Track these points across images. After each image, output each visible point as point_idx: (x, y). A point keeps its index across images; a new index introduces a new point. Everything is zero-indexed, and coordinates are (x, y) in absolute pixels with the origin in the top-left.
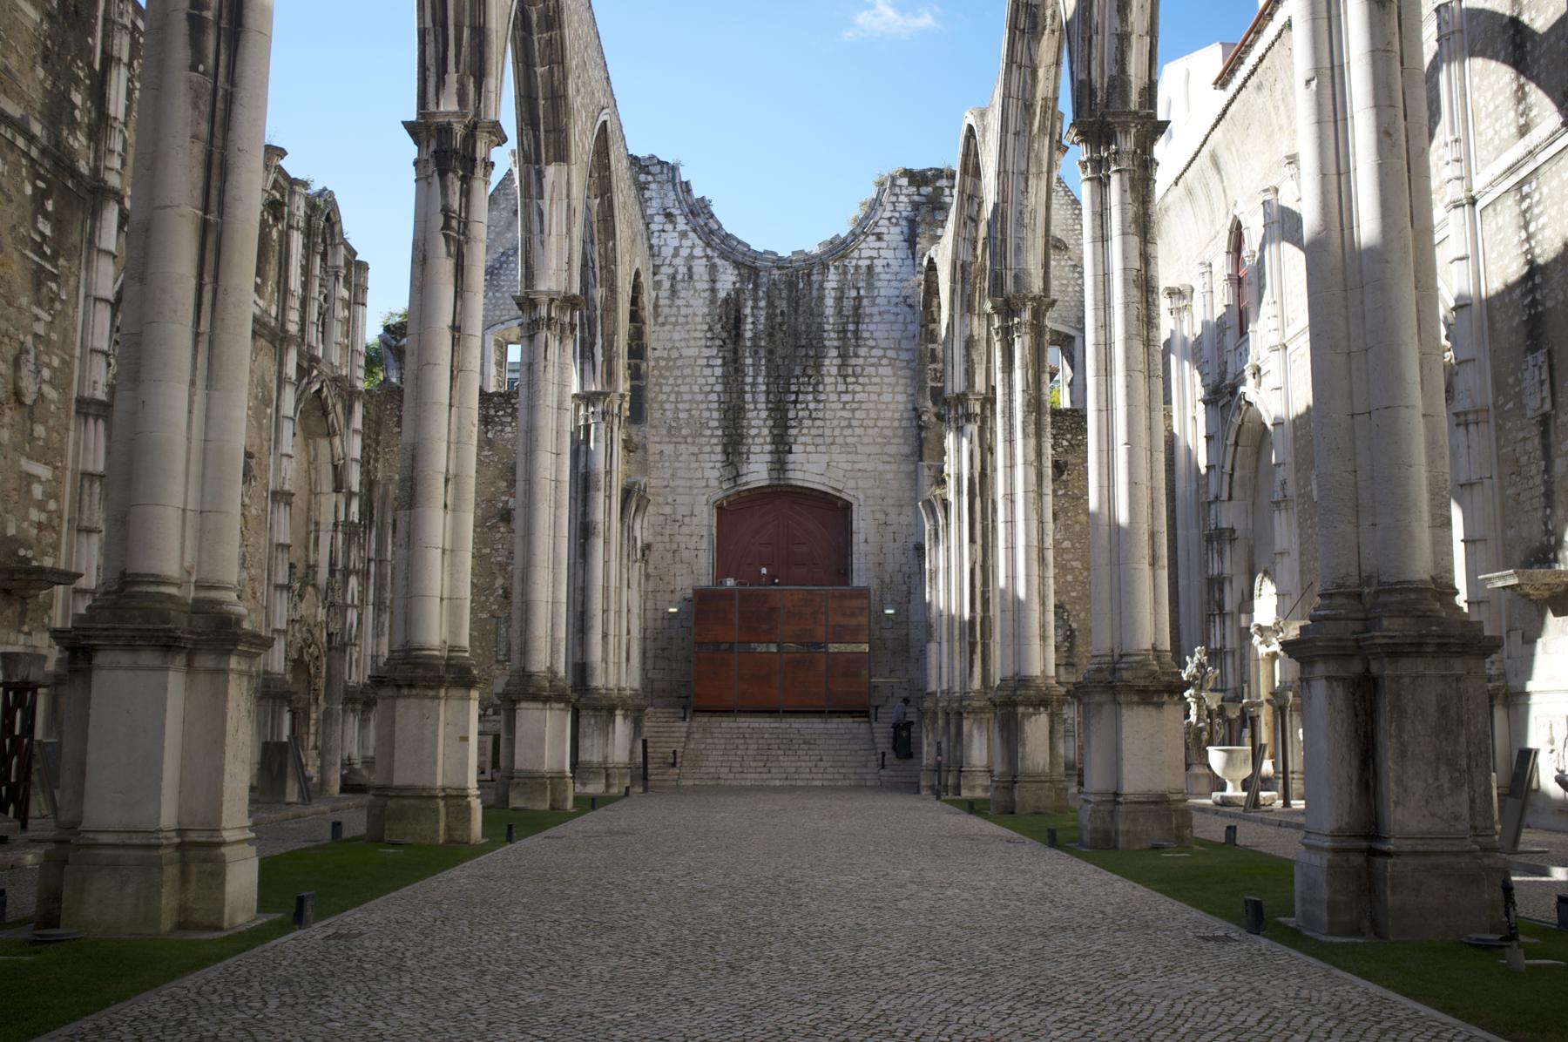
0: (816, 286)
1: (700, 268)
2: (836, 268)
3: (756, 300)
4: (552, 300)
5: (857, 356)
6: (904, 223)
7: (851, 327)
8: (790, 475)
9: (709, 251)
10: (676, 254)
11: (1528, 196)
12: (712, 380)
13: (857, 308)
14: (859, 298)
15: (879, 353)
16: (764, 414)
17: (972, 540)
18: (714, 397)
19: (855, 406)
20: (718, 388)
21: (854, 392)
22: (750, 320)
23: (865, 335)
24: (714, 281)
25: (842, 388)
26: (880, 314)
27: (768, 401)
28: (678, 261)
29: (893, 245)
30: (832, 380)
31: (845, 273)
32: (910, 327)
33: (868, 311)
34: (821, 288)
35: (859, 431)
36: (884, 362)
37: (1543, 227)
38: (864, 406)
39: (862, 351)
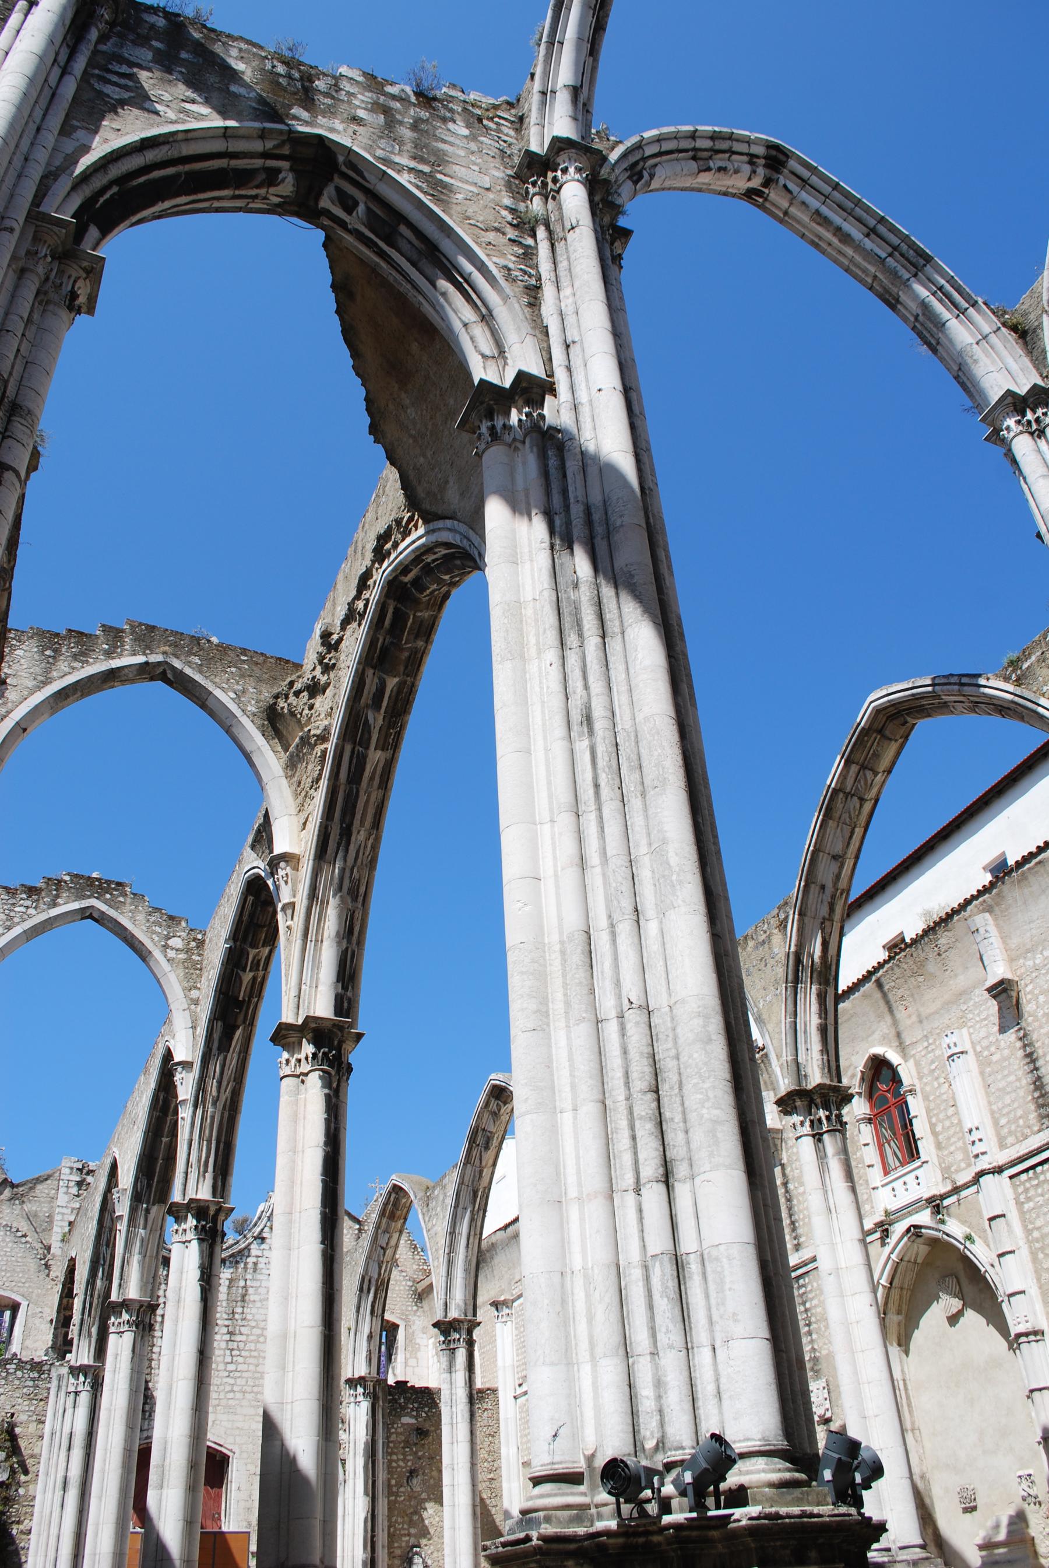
4: (141, 1306)
11: (803, 1286)
13: (244, 1296)
15: (259, 1332)
17: (366, 1493)
21: (237, 1363)
23: (249, 1317)
25: (228, 1359)
30: (222, 1352)
33: (252, 1298)
37: (816, 1306)
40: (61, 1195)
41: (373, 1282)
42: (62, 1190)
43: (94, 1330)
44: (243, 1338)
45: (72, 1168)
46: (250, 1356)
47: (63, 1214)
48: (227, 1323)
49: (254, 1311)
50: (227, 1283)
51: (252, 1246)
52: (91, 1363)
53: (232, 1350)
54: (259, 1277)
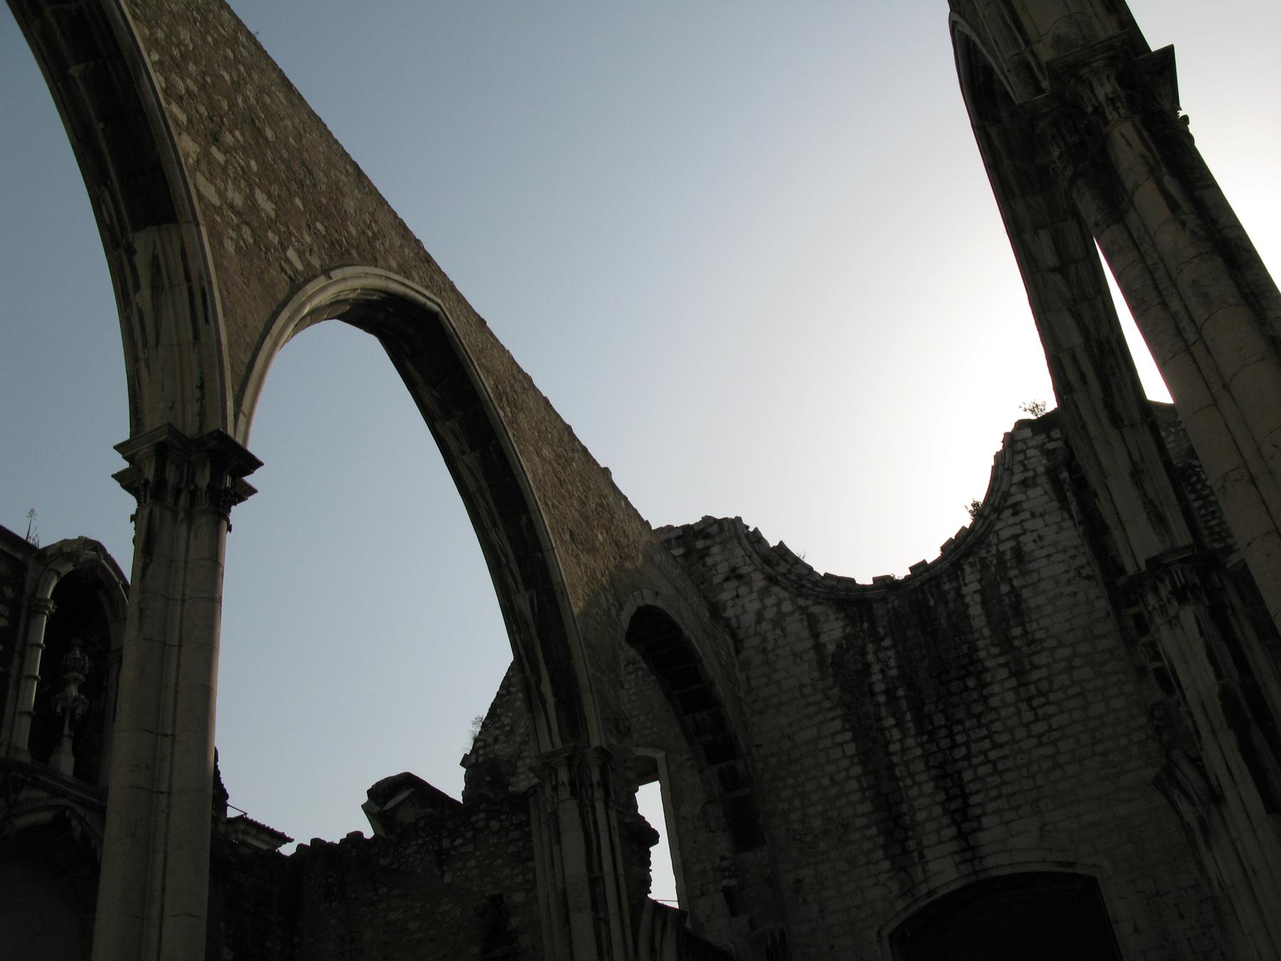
0: (952, 595)
1: (795, 625)
2: (972, 565)
3: (877, 640)
7: (1017, 631)
8: (990, 862)
9: (801, 602)
10: (760, 618)
12: (845, 763)
14: (1014, 592)
15: (1066, 652)
16: (928, 788)
18: (853, 785)
20: (856, 770)
21: (1047, 718)
22: (876, 668)
23: (1039, 635)
24: (815, 635)
25: (1028, 716)
27: (929, 768)
28: (765, 626)
30: (1012, 710)
33: (1032, 603)
34: (960, 596)
36: (1077, 662)
41: (1082, 356)
44: (1043, 672)
48: (1002, 660)
50: (978, 598)
53: (1029, 700)
54: (1031, 566)
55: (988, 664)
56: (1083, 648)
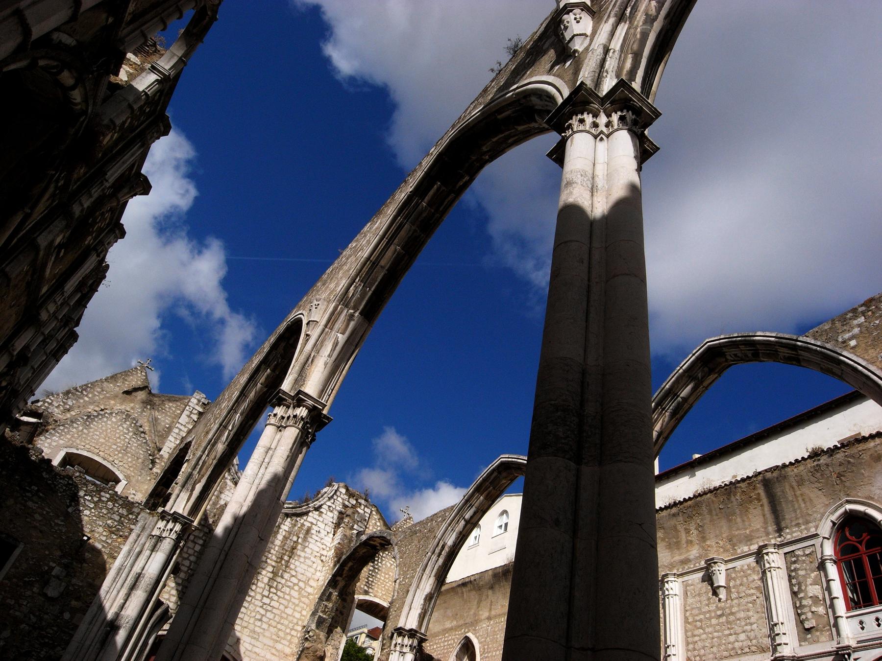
5: (282, 577)
6: (336, 513)
7: (286, 558)
12: (191, 551)
13: (294, 548)
14: (296, 542)
19: (269, 608)
21: (272, 599)
23: (292, 566)
25: (266, 593)
26: (305, 558)
29: (325, 522)
30: (263, 585)
31: (295, 525)
32: (318, 574)
33: (299, 553)
35: (265, 626)
36: (296, 588)
38: (274, 611)
39: (286, 576)
40: (184, 416)
42: (186, 413)
43: (199, 487)
44: (283, 581)
45: (199, 401)
46: (284, 598)
47: (180, 430)
48: (274, 564)
49: (297, 563)
51: (310, 514)
52: (185, 514)
55: (268, 560)
56: (301, 584)
